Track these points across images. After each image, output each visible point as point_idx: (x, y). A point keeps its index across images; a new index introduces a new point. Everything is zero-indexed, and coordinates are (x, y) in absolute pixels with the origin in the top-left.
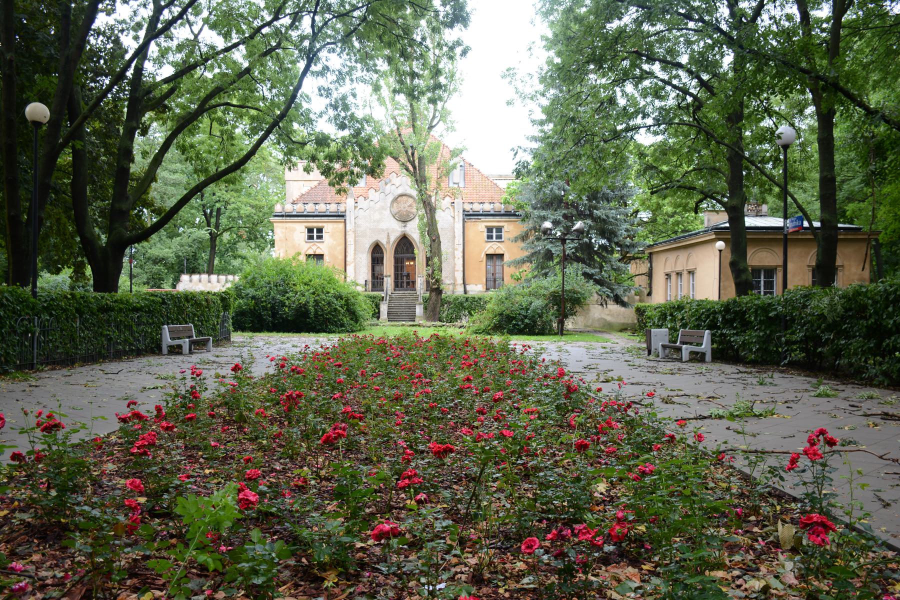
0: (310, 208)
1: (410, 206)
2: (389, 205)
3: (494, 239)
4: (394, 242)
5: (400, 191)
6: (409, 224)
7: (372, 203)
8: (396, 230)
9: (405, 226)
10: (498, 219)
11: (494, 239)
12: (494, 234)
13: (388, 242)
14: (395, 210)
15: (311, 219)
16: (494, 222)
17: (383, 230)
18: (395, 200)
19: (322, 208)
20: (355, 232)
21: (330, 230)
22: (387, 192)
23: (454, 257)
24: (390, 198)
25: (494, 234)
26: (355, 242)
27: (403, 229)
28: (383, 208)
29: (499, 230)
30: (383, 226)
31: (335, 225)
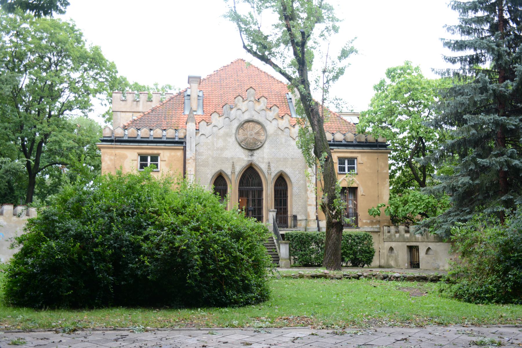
0: (143, 133)
1: (258, 133)
2: (234, 131)
4: (240, 172)
5: (246, 117)
6: (257, 153)
7: (215, 129)
8: (241, 159)
9: (252, 155)
10: (351, 149)
12: (346, 166)
13: (233, 173)
14: (241, 137)
16: (346, 153)
17: (227, 159)
18: (241, 126)
19: (157, 133)
20: (195, 160)
21: (166, 158)
22: (232, 117)
23: (306, 191)
24: (236, 124)
25: (346, 166)
26: (196, 171)
27: (250, 159)
28: (227, 135)
29: (352, 161)
30: (228, 154)
31: (173, 153)
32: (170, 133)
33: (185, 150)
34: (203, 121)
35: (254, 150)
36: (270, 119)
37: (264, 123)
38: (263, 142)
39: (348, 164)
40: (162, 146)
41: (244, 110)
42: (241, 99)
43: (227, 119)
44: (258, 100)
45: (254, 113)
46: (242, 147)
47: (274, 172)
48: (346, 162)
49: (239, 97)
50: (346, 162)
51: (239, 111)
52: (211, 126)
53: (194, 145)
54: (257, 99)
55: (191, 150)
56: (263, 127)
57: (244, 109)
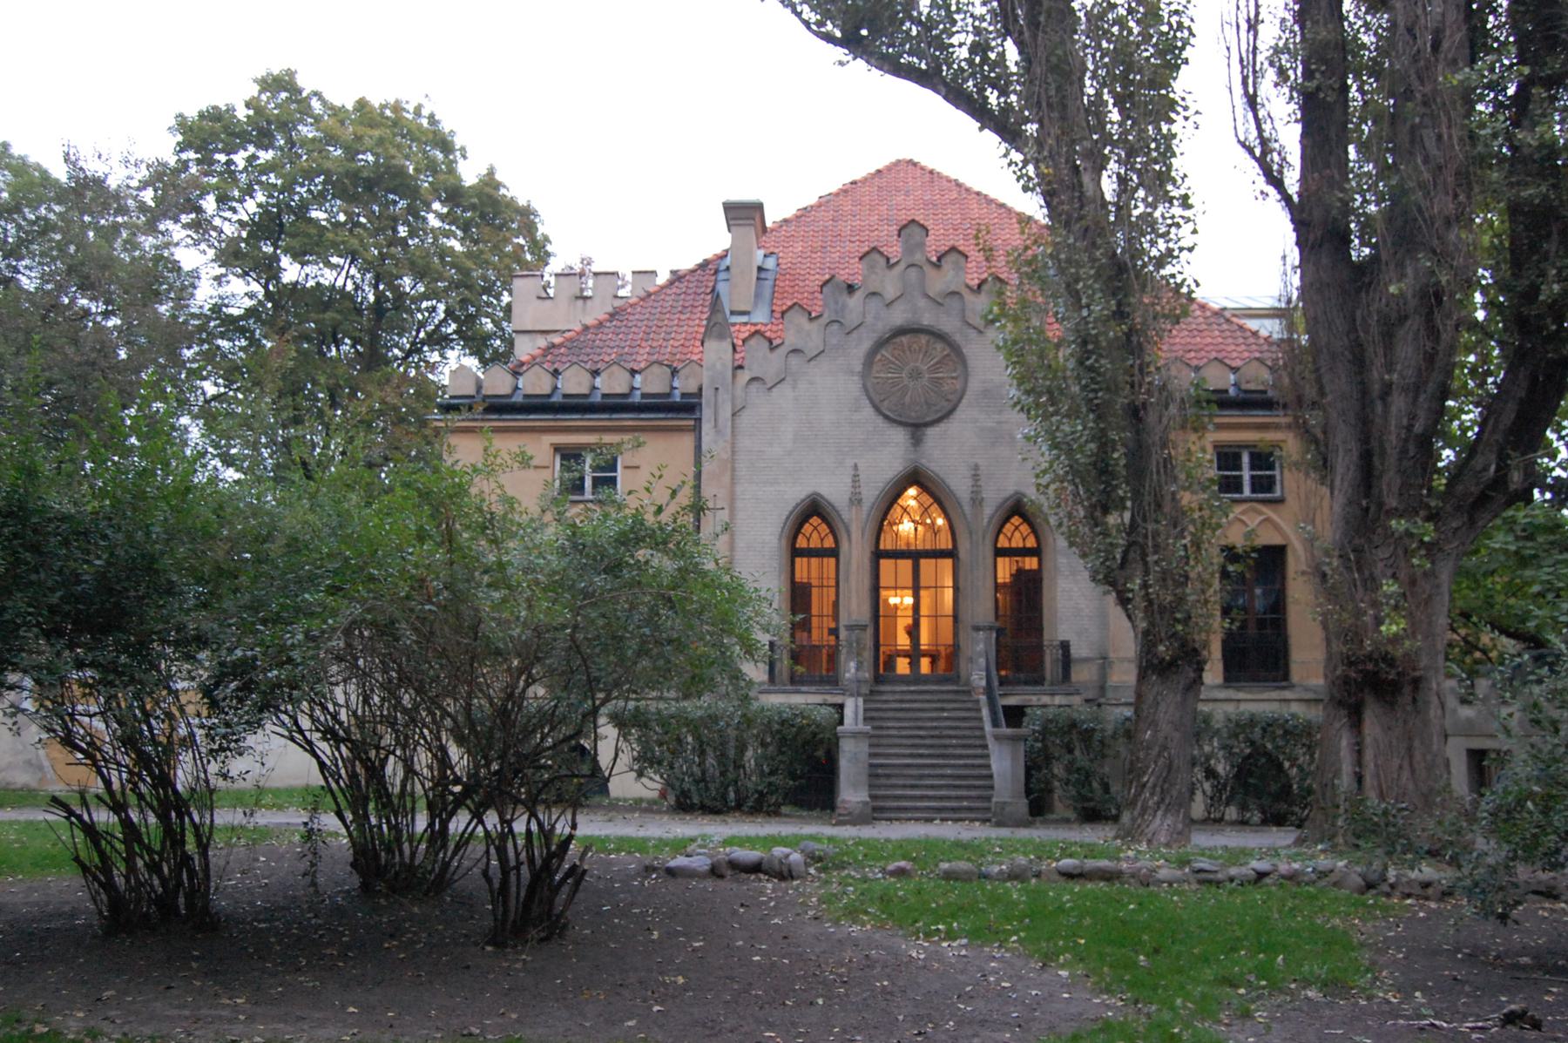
0: (574, 383)
3: (1247, 491)
5: (898, 317)
10: (1259, 417)
11: (1247, 491)
12: (1246, 474)
13: (856, 500)
15: (574, 420)
16: (1244, 432)
19: (612, 383)
22: (852, 319)
25: (1246, 474)
32: (651, 383)
33: (697, 429)
34: (757, 337)
35: (927, 425)
36: (979, 322)
37: (957, 338)
38: (953, 397)
39: (1252, 468)
40: (627, 420)
42: (882, 261)
43: (835, 327)
44: (937, 265)
45: (922, 303)
46: (886, 417)
48: (1246, 459)
49: (875, 256)
50: (1246, 459)
51: (874, 300)
52: (782, 351)
53: (726, 412)
54: (934, 259)
56: (956, 349)
57: (890, 291)
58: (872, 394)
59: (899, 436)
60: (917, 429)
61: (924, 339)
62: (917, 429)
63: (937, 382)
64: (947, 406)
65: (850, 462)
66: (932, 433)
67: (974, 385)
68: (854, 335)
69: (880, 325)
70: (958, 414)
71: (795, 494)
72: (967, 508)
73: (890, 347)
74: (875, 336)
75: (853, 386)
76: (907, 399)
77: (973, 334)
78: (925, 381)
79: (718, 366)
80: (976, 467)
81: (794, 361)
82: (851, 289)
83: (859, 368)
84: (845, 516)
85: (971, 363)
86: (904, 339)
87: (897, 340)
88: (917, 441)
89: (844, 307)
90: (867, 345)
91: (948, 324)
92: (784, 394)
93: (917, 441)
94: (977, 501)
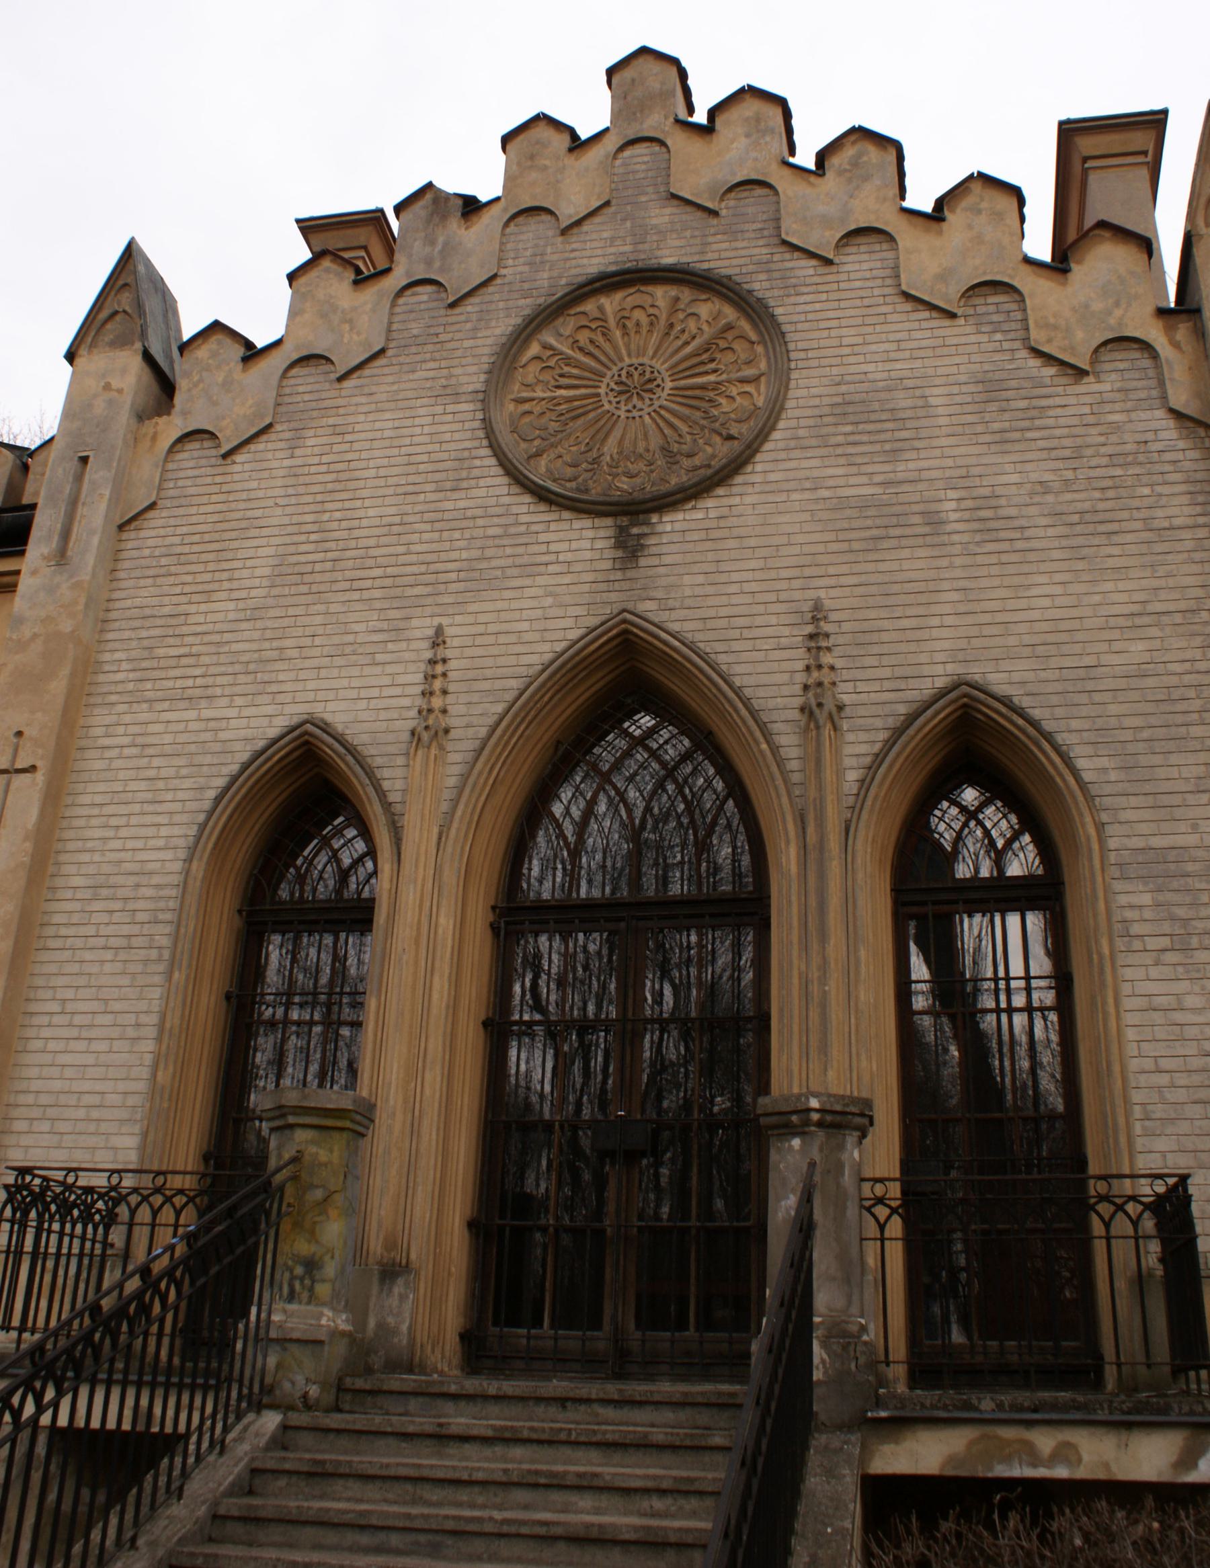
5: (596, 253)
36: (822, 239)
37: (759, 285)
41: (569, 210)
45: (661, 216)
46: (542, 495)
47: (882, 694)
53: (95, 515)
55: (61, 556)
58: (506, 439)
59: (584, 542)
60: (630, 516)
61: (661, 294)
62: (630, 516)
63: (697, 399)
64: (722, 451)
65: (423, 627)
66: (671, 523)
67: (808, 390)
68: (471, 307)
69: (543, 279)
70: (764, 468)
71: (252, 724)
72: (789, 741)
73: (567, 325)
74: (526, 305)
75: (458, 428)
76: (610, 447)
77: (807, 268)
78: (663, 397)
79: (99, 408)
80: (818, 613)
81: (307, 381)
82: (470, 206)
83: (472, 377)
84: (393, 779)
85: (797, 340)
86: (610, 304)
87: (589, 306)
88: (629, 549)
89: (449, 249)
90: (503, 326)
91: (724, 255)
92: (263, 474)
93: (629, 549)
94: (819, 712)
